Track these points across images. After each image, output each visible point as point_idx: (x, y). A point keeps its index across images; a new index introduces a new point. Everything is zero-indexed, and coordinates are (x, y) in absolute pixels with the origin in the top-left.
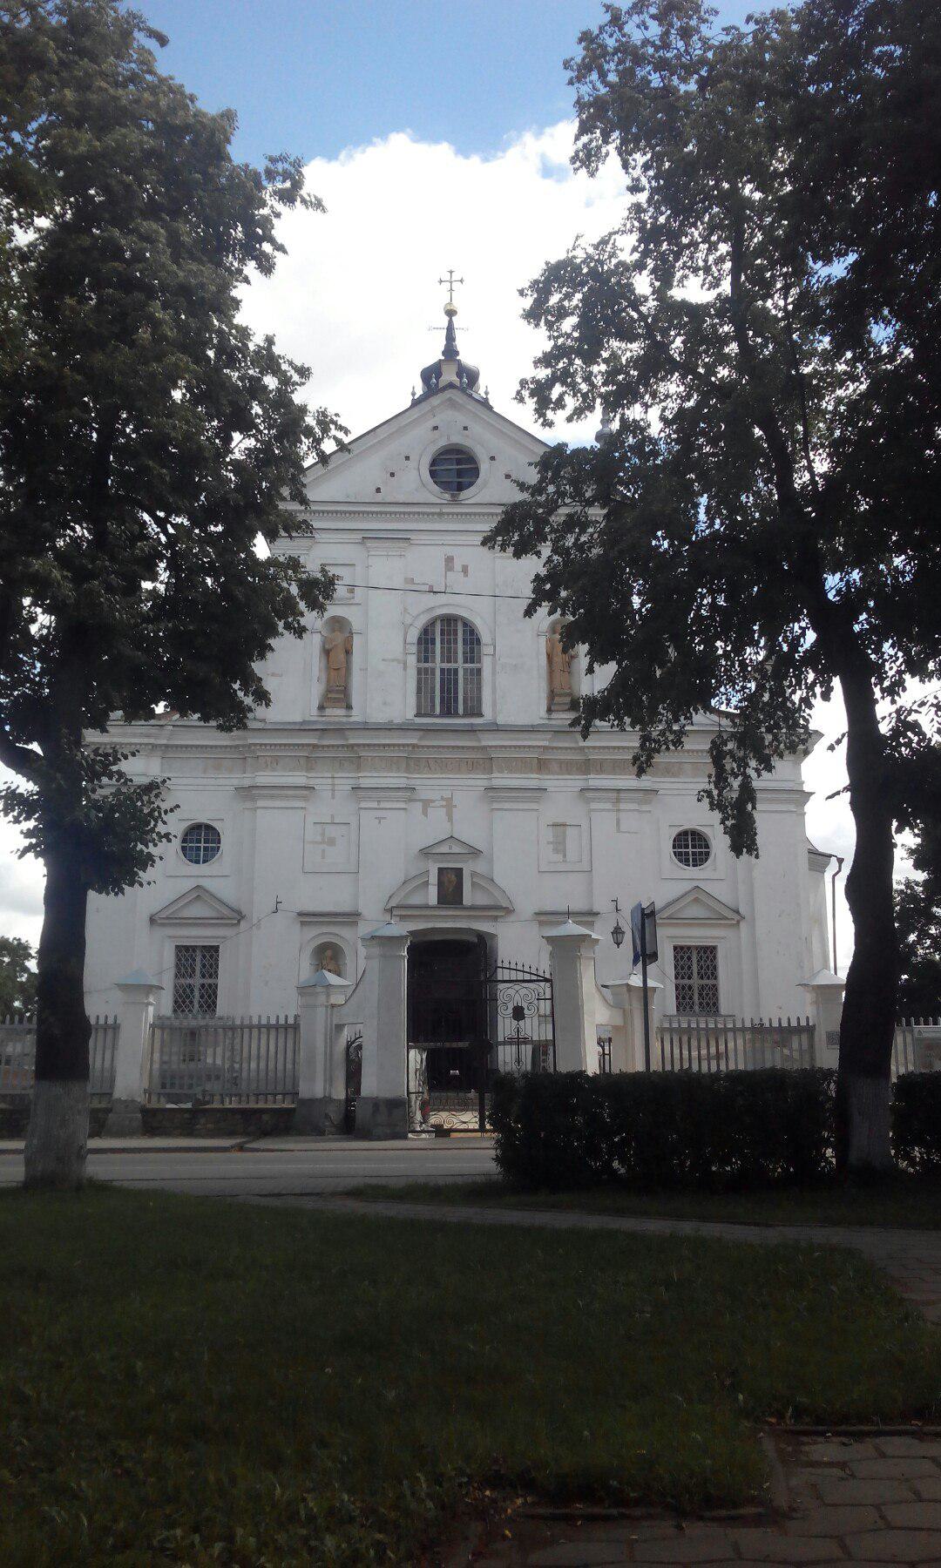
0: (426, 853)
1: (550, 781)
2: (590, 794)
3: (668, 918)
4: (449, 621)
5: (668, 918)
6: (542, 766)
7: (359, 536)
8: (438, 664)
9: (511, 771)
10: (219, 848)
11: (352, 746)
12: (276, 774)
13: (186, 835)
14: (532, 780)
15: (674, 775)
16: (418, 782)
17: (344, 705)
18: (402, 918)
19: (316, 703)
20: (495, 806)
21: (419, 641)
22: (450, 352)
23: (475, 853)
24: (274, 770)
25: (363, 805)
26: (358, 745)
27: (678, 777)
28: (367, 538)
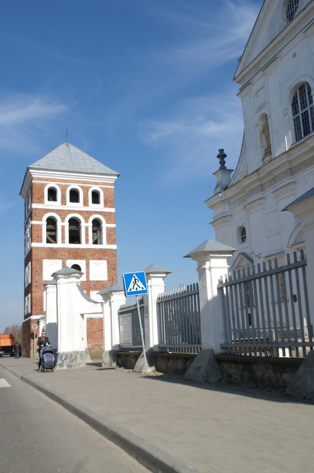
10: (242, 235)
12: (254, 196)
13: (242, 233)
17: (269, 154)
19: (261, 159)
21: (293, 106)
24: (252, 196)
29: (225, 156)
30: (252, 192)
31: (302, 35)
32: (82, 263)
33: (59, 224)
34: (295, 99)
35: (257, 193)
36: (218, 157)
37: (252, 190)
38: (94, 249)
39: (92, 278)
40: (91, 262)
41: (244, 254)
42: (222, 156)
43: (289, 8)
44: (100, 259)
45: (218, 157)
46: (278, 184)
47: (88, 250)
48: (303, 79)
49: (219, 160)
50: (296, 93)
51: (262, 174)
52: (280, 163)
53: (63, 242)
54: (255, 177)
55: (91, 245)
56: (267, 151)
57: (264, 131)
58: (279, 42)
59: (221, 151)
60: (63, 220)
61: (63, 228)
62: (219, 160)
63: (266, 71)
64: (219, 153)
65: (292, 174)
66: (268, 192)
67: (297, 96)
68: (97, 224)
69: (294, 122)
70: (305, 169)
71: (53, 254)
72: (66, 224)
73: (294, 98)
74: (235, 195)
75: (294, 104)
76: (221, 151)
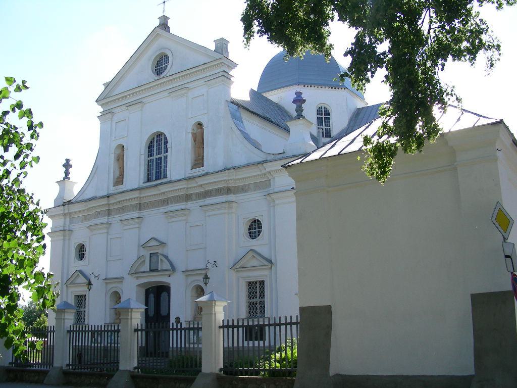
0: (144, 246)
1: (190, 205)
2: (205, 208)
3: (240, 268)
4: (159, 135)
5: (240, 268)
6: (188, 198)
7: (124, 107)
8: (155, 157)
9: (175, 203)
11: (119, 202)
14: (182, 205)
15: (246, 192)
16: (144, 214)
18: (137, 278)
20: (170, 220)
23: (162, 244)
24: (98, 217)
25: (125, 228)
26: (121, 201)
27: (248, 192)
28: (129, 105)
29: (71, 166)
30: (98, 214)
31: (166, 94)
35: (103, 217)
36: (64, 166)
37: (99, 213)
41: (80, 271)
42: (67, 165)
43: (158, 64)
45: (64, 166)
46: (125, 214)
48: (161, 130)
49: (64, 169)
50: (154, 138)
51: (112, 201)
52: (131, 197)
54: (105, 201)
56: (119, 180)
58: (146, 89)
59: (68, 161)
62: (64, 169)
63: (130, 108)
64: (65, 162)
65: (140, 209)
66: (115, 219)
67: (154, 141)
69: (148, 163)
70: (153, 208)
73: (151, 142)
74: (79, 211)
75: (150, 147)
76: (68, 161)
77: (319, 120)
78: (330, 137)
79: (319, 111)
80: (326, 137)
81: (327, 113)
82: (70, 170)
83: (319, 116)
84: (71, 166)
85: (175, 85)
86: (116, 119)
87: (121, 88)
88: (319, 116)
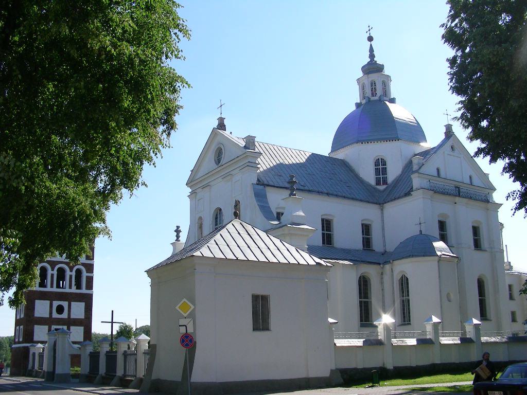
22: (372, 56)
29: (180, 231)
31: (220, 179)
32: (65, 304)
33: (50, 272)
34: (217, 215)
36: (175, 231)
38: (75, 293)
39: (72, 316)
40: (73, 303)
42: (178, 231)
44: (80, 301)
45: (175, 231)
47: (71, 294)
53: (52, 287)
55: (74, 290)
57: (200, 228)
59: (178, 227)
60: (53, 270)
61: (52, 275)
63: (204, 189)
68: (79, 272)
71: (44, 296)
72: (55, 272)
76: (178, 227)
77: (377, 171)
78: (387, 184)
79: (377, 163)
80: (383, 184)
81: (384, 163)
82: (180, 234)
83: (385, 167)
84: (180, 231)
85: (223, 174)
86: (198, 197)
87: (200, 174)
88: (385, 167)
